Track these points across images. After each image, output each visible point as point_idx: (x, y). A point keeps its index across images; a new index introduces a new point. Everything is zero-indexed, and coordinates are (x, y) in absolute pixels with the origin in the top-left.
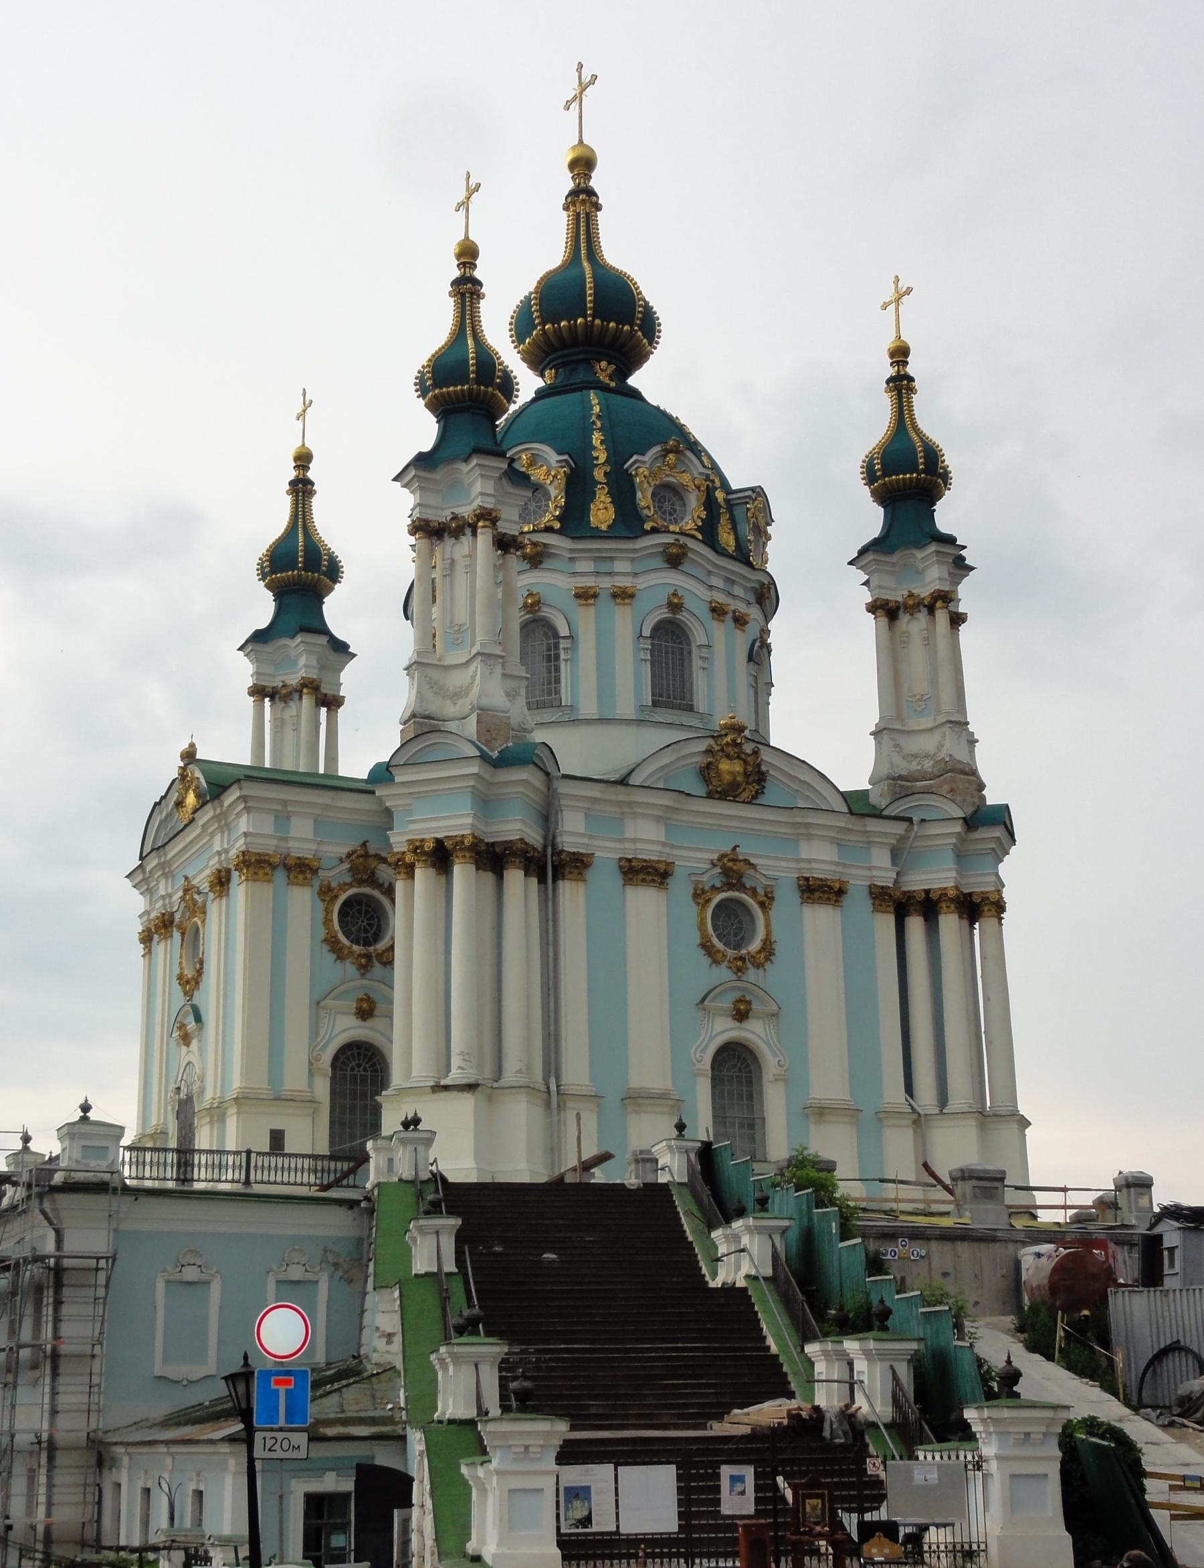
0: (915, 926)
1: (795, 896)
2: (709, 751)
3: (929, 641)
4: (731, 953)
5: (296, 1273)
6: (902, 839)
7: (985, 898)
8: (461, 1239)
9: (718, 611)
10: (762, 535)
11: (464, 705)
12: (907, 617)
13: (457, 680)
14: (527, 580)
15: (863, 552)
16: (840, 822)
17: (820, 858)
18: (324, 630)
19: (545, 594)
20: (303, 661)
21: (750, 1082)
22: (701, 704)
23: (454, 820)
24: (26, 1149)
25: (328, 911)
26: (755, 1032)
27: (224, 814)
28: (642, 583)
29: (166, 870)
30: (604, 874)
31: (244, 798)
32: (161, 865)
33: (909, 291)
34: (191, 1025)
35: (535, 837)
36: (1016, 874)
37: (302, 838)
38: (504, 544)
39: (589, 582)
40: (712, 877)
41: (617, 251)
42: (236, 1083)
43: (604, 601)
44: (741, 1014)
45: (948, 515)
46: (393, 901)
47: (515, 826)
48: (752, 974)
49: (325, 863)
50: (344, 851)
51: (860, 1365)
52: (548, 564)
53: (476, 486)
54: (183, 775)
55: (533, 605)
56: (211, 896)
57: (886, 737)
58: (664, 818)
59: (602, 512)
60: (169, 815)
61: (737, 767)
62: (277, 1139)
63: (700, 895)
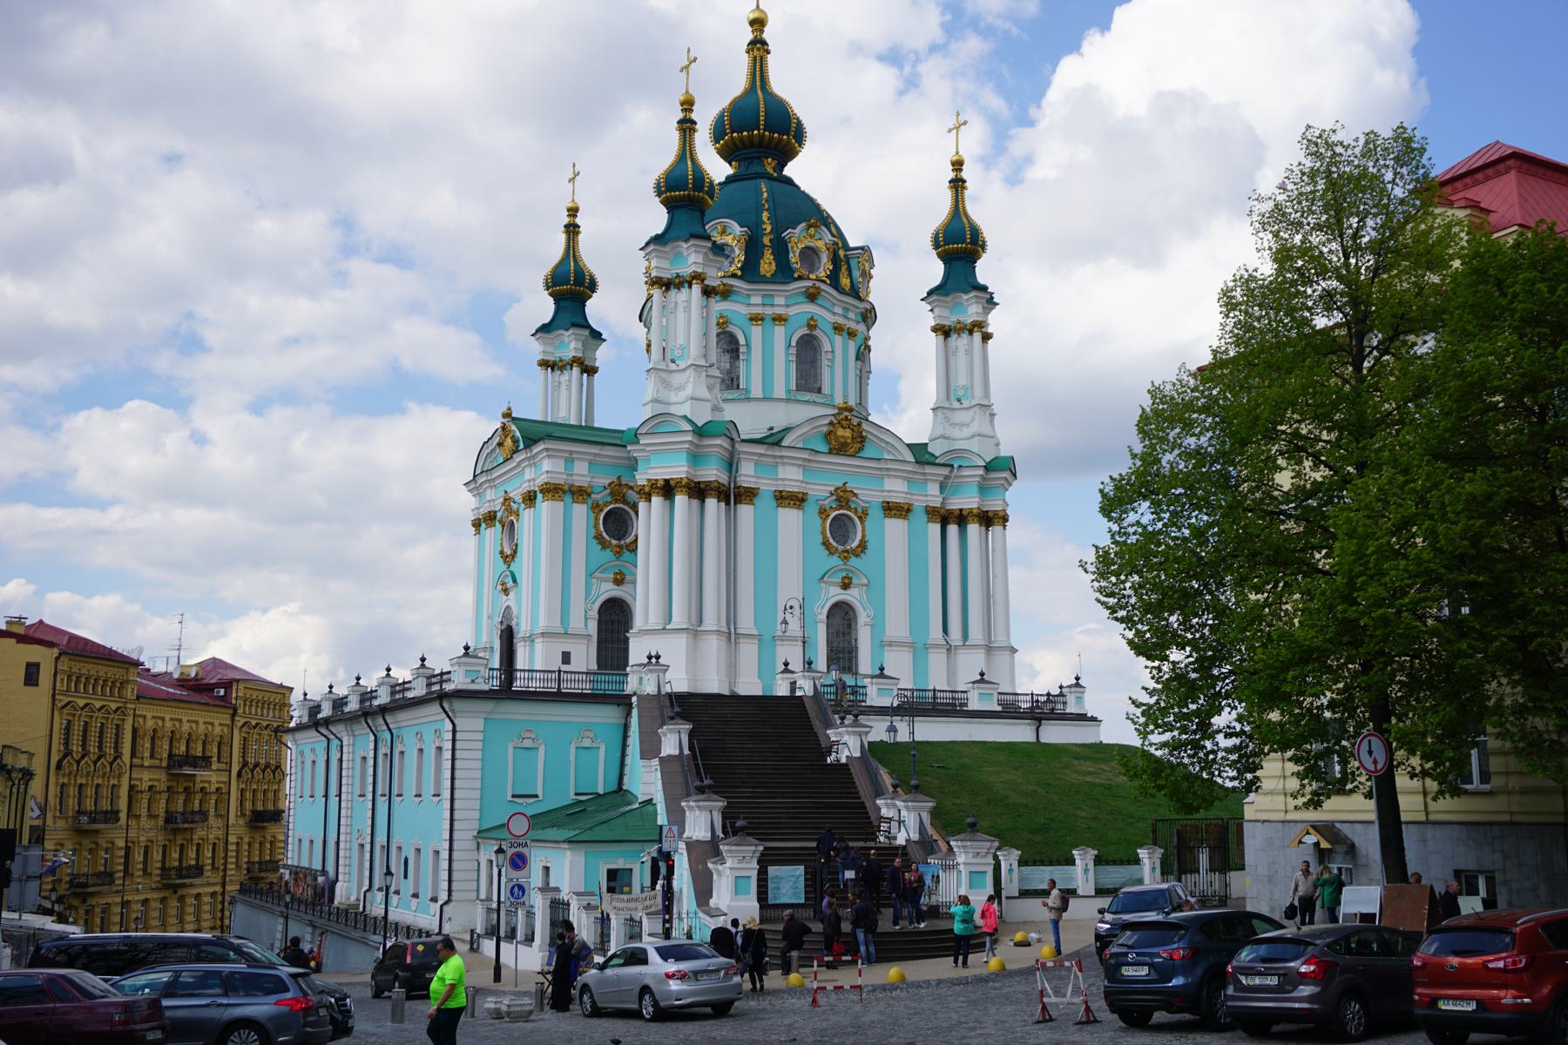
0: (953, 529)
1: (881, 514)
2: (831, 423)
3: (969, 352)
4: (841, 548)
5: (587, 743)
6: (947, 477)
7: (996, 513)
8: (691, 735)
9: (838, 329)
10: (867, 276)
11: (683, 395)
13: (677, 379)
14: (719, 306)
15: (930, 293)
17: (896, 489)
18: (588, 326)
19: (730, 315)
20: (573, 345)
21: (849, 626)
22: (826, 390)
23: (675, 468)
24: (423, 666)
25: (597, 519)
26: (853, 596)
27: (534, 457)
28: (792, 311)
30: (765, 501)
33: (965, 123)
34: (510, 583)
35: (723, 478)
36: (1016, 498)
37: (581, 473)
38: (708, 292)
39: (759, 310)
40: (830, 502)
41: (782, 83)
42: (542, 624)
43: (768, 322)
44: (846, 585)
45: (984, 271)
46: (637, 513)
47: (712, 473)
48: (853, 561)
49: (596, 490)
51: (904, 813)
52: (733, 297)
53: (691, 258)
54: (504, 428)
55: (723, 323)
57: (939, 412)
58: (805, 466)
59: (767, 265)
61: (848, 433)
62: (566, 658)
63: (823, 512)
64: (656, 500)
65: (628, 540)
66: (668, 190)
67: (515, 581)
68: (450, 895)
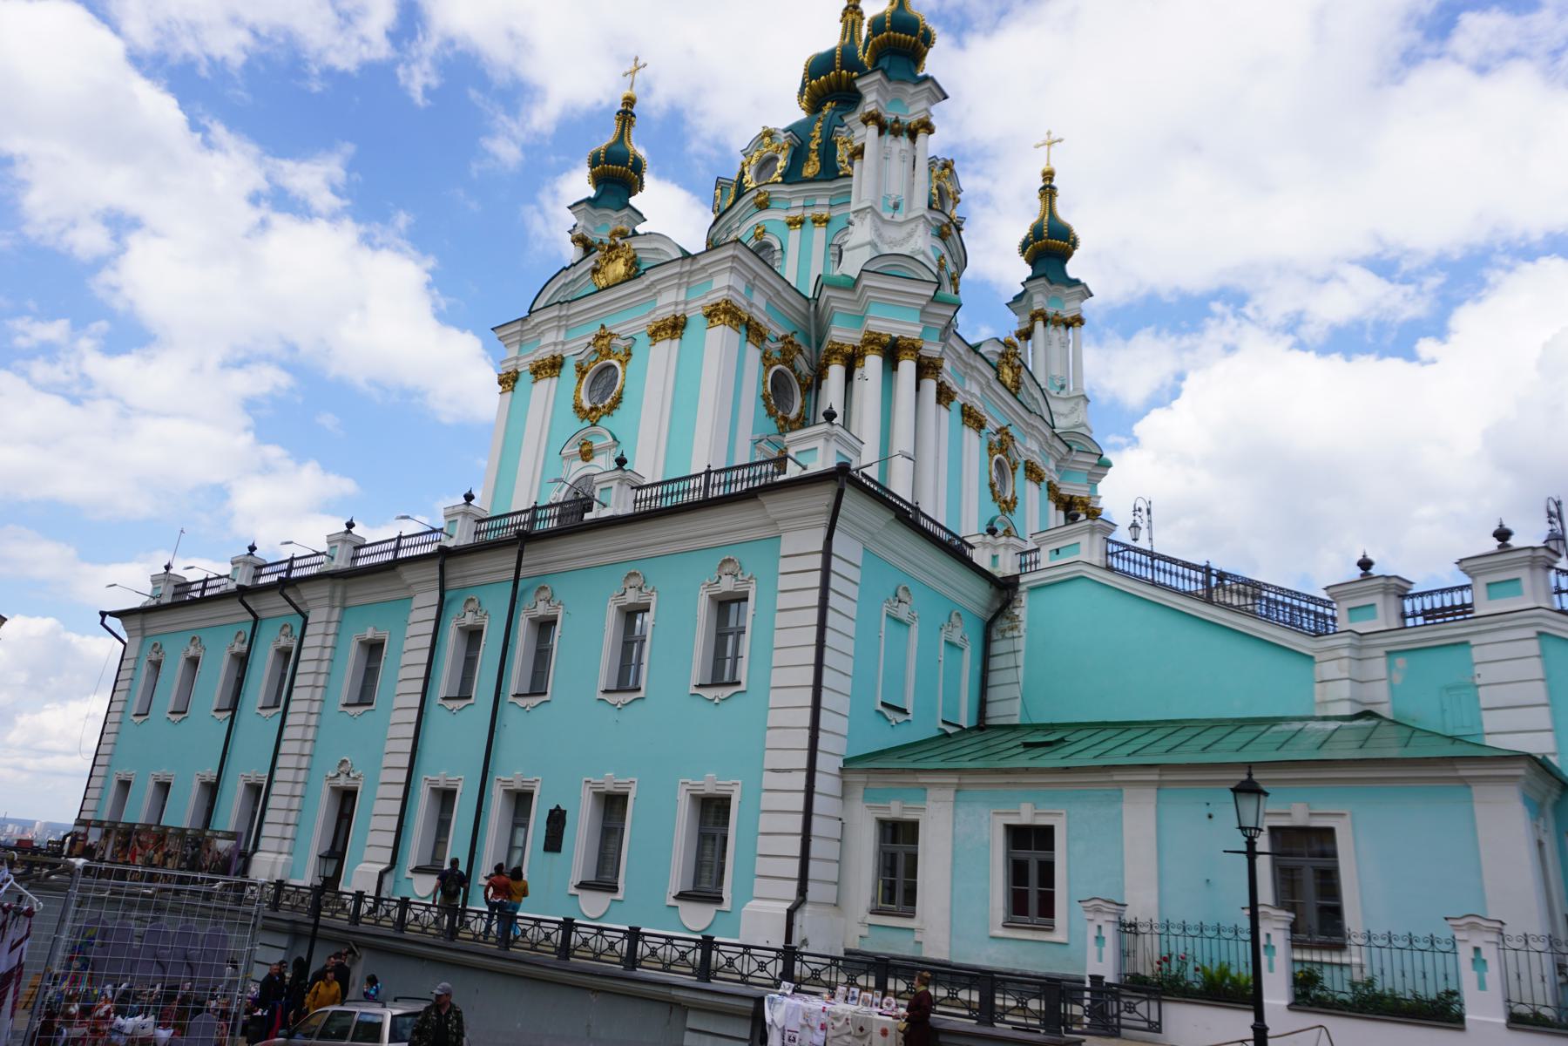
2: (1002, 355)
5: (956, 639)
12: (1051, 327)
16: (1048, 432)
25: (766, 373)
27: (691, 273)
29: (562, 323)
31: (734, 257)
32: (560, 318)
37: (758, 307)
50: (781, 334)
56: (643, 340)
60: (574, 281)
64: (873, 363)
65: (793, 415)
66: (894, 28)
67: (615, 439)
68: (802, 890)
